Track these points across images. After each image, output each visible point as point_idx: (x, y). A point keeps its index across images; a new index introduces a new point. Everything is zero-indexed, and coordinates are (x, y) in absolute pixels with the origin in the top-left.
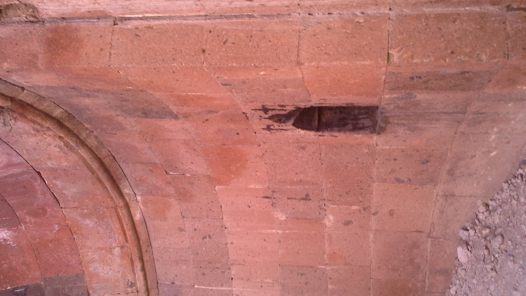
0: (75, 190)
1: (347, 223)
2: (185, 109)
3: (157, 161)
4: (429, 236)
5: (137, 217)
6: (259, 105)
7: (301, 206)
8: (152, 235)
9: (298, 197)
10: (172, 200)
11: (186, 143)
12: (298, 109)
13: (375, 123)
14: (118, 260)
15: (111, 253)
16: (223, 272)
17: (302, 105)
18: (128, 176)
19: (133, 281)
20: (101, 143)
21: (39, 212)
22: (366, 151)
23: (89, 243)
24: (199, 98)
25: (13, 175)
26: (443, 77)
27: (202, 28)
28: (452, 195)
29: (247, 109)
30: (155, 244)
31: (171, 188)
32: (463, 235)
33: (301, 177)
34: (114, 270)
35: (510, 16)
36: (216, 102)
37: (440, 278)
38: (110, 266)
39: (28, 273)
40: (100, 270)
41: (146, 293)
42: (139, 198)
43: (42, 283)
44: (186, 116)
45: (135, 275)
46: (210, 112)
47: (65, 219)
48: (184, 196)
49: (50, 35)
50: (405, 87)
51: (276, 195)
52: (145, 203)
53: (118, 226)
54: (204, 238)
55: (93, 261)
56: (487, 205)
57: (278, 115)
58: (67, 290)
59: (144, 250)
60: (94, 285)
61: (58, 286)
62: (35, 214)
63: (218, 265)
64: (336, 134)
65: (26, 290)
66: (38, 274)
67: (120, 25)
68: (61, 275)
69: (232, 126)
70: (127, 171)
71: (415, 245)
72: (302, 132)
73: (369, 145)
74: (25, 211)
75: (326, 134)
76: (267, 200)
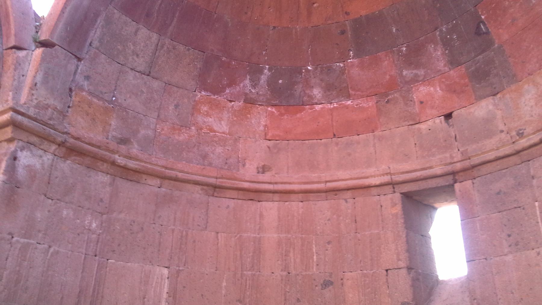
19: (525, 134)
34: (532, 111)
38: (536, 104)
39: (504, 27)
40: (528, 97)
41: (514, 152)
43: (496, 45)
45: (534, 133)
58: (495, 71)
60: (508, 96)
61: (497, 62)
65: (484, 33)
66: (505, 37)
68: (511, 60)
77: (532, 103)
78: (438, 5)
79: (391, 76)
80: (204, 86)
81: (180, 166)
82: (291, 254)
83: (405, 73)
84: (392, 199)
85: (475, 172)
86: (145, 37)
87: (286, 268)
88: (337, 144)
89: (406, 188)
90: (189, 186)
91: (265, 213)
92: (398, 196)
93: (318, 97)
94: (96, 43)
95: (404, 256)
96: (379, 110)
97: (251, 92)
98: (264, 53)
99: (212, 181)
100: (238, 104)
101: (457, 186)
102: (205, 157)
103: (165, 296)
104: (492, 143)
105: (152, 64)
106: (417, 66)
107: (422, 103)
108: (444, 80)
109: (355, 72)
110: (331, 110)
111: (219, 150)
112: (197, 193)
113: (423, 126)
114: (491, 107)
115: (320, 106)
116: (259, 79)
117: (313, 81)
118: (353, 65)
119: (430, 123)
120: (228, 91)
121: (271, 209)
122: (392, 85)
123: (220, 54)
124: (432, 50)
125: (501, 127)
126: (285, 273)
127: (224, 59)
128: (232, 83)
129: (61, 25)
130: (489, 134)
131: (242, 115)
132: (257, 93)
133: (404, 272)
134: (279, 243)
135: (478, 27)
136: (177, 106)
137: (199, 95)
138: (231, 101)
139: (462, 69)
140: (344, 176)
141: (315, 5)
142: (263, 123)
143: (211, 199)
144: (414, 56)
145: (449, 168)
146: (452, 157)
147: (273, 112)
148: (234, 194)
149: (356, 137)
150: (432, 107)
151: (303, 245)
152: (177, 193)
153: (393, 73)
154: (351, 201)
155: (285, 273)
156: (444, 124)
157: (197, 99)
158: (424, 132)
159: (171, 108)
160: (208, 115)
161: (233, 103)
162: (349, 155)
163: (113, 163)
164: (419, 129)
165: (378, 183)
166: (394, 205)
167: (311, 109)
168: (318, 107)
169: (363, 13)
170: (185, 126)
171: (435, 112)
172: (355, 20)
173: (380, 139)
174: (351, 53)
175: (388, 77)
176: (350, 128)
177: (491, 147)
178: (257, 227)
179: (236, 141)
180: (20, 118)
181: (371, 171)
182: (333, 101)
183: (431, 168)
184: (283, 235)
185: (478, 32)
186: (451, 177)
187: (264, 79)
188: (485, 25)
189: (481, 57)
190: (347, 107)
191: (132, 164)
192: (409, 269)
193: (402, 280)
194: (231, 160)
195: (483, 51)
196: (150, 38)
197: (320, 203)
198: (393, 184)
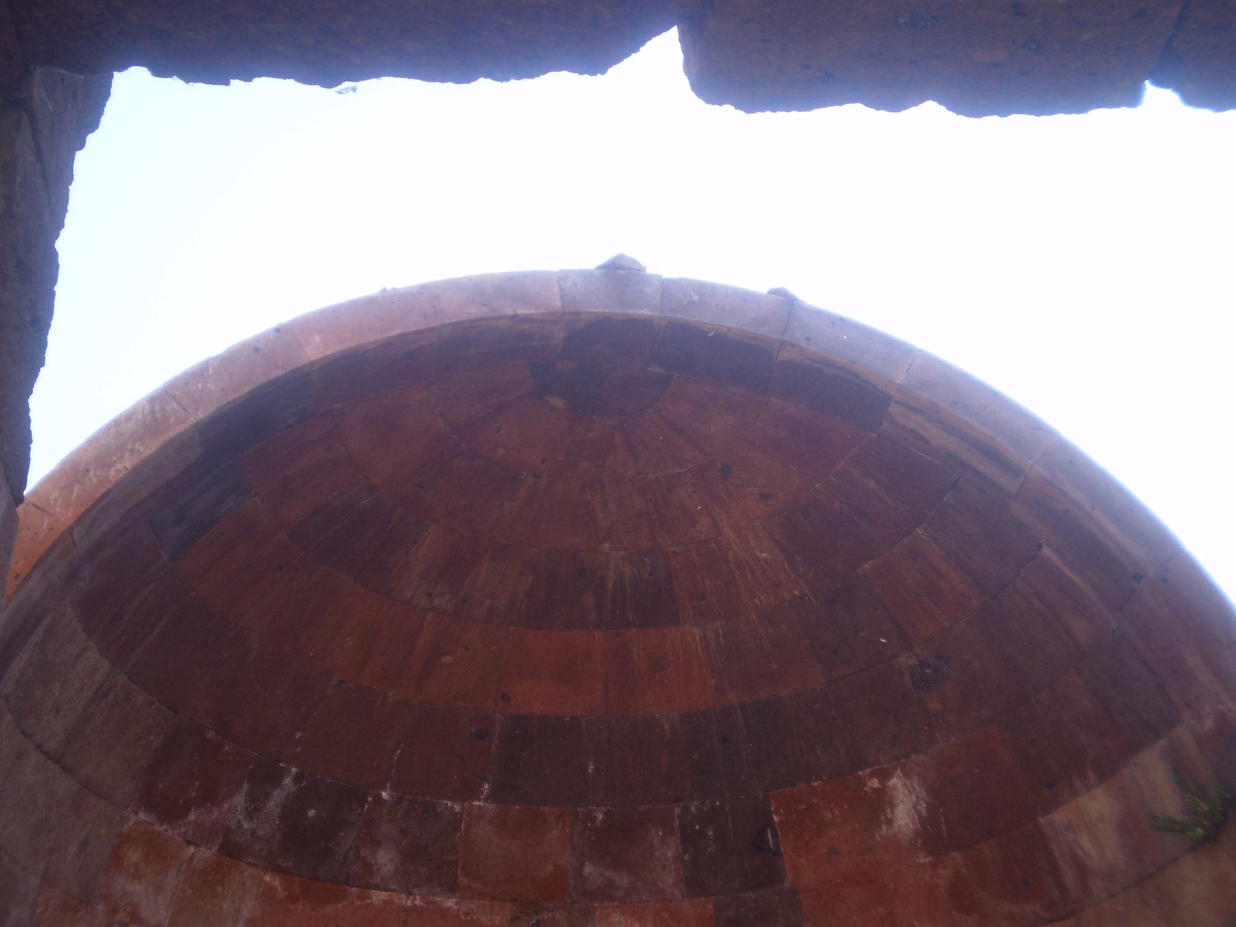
74: (964, 871)
78: (695, 756)
83: (588, 869)
93: (384, 871)
97: (240, 826)
98: (298, 735)
100: (206, 854)
108: (666, 915)
110: (408, 911)
132: (253, 833)
137: (133, 818)
138: (189, 843)
141: (445, 659)
142: (246, 914)
147: (274, 889)
157: (125, 828)
161: (192, 849)
167: (362, 898)
168: (378, 897)
174: (486, 786)
175: (550, 867)
182: (415, 891)
187: (277, 797)
188: (775, 835)
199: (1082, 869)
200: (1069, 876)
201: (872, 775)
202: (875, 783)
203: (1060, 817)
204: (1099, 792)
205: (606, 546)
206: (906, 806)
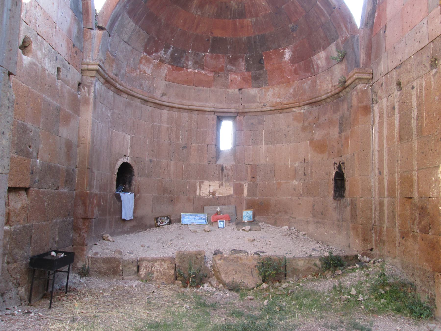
0: (306, 87)
1: (294, 189)
2: (343, 138)
3: (320, 121)
4: (290, 217)
5: (294, 109)
6: (345, 161)
7: (301, 172)
8: (286, 114)
9: (305, 172)
10: (301, 124)
11: (328, 134)
12: (344, 174)
13: (337, 197)
14: (274, 100)
15: (278, 98)
16: (270, 142)
17: (345, 175)
18: (312, 108)
20: (328, 102)
21: (296, 72)
22: (326, 195)
23: (282, 89)
24: (348, 144)
25: (313, 66)
26: (355, 212)
27: (370, 150)
28: (308, 224)
29: (343, 157)
30: (281, 115)
31: (307, 124)
32: (293, 228)
33: (314, 173)
35: (372, 225)
36: (346, 149)
37: (273, 221)
40: (270, 93)
42: (302, 111)
44: (340, 137)
46: (342, 145)
47: (293, 81)
48: (304, 129)
49: (368, 107)
50: (352, 203)
51: (306, 163)
52: (300, 113)
53: (291, 102)
54: (285, 135)
55: (274, 90)
56: (305, 235)
57: (341, 167)
59: (280, 111)
60: (263, 90)
62: (296, 71)
63: (273, 140)
64: (333, 185)
66: (269, 68)
67: (371, 127)
68: (268, 77)
69: (336, 151)
70: (314, 108)
71: (286, 212)
72: (334, 174)
73: (328, 195)
75: (333, 182)
76: (303, 160)
77: (271, 96)
79: (222, 66)
80: (146, 51)
81: (135, 90)
82: (172, 134)
83: (228, 66)
84: (213, 118)
85: (245, 114)
86: (131, 25)
87: (170, 139)
88: (194, 89)
89: (219, 114)
90: (136, 99)
91: (162, 115)
92: (215, 117)
94: (116, 28)
95: (214, 140)
96: (214, 78)
99: (145, 98)
100: (157, 61)
101: (238, 117)
102: (141, 85)
103: (129, 146)
104: (255, 105)
105: (130, 38)
106: (234, 65)
107: (231, 81)
109: (208, 59)
110: (195, 73)
111: (147, 82)
112: (138, 102)
113: (230, 91)
114: (256, 92)
115: (190, 70)
116: (168, 51)
117: (190, 58)
118: (208, 56)
119: (233, 90)
120: (154, 54)
121: (165, 113)
122: (222, 70)
123: (155, 37)
124: (241, 61)
125: (258, 100)
126: (169, 142)
127: (156, 39)
128: (157, 51)
129: (109, 21)
130: (254, 102)
131: (158, 67)
133: (214, 146)
134: (168, 128)
135: (261, 60)
136: (134, 59)
139: (250, 73)
140: (196, 105)
141: (200, 25)
143: (143, 106)
144: (233, 61)
145: (237, 111)
146: (239, 107)
148: (152, 105)
149: (202, 88)
150: (235, 84)
151: (176, 131)
152: (132, 102)
153: (223, 65)
154: (197, 115)
155: (169, 142)
156: (238, 92)
158: (230, 93)
159: (132, 60)
160: (144, 65)
162: (199, 95)
163: (116, 87)
164: (228, 92)
165: (209, 110)
166: (213, 120)
168: (189, 70)
169: (219, 36)
170: (136, 69)
171: (236, 86)
172: (215, 37)
173: (212, 91)
175: (221, 66)
176: (200, 83)
177: (254, 107)
178: (159, 121)
179: (153, 79)
180: (100, 69)
181: (207, 104)
183: (230, 109)
184: (169, 126)
185: (260, 62)
186: (236, 114)
187: (169, 51)
189: (258, 71)
190: (201, 73)
191: (121, 88)
192: (216, 145)
193: (213, 148)
194: (151, 88)
195: (260, 70)
196: (132, 26)
197: (184, 114)
198: (215, 112)
199: (318, 67)
200: (316, 68)
201: (282, 49)
202: (282, 51)
203: (315, 57)
204: (323, 52)
205: (232, 1)
206: (288, 55)
